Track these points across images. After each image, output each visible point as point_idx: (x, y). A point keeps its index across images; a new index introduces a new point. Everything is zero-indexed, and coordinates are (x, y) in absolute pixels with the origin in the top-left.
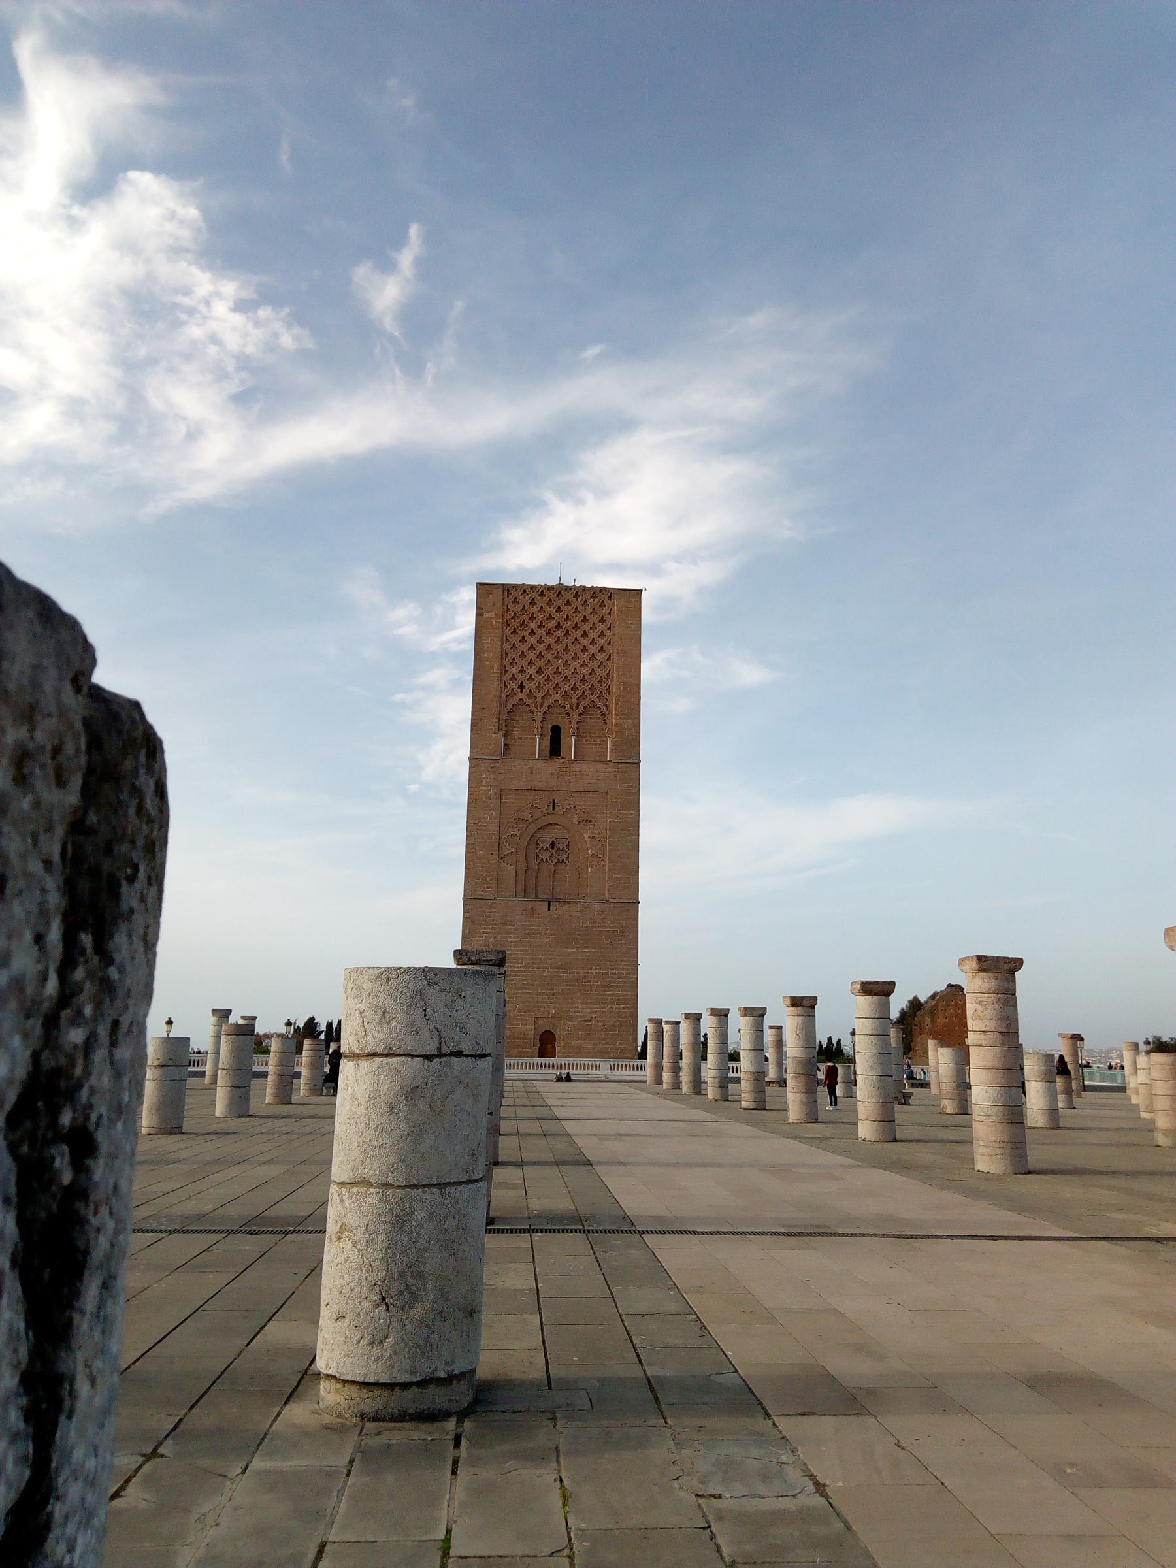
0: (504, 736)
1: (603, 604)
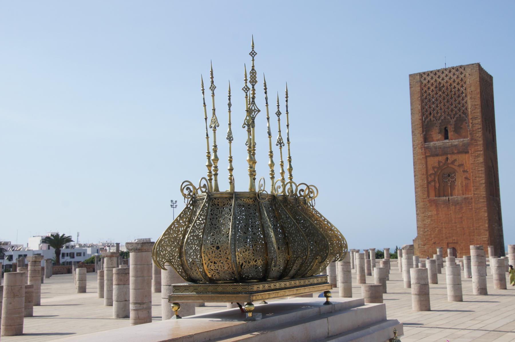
0: (425, 135)
1: (461, 73)
